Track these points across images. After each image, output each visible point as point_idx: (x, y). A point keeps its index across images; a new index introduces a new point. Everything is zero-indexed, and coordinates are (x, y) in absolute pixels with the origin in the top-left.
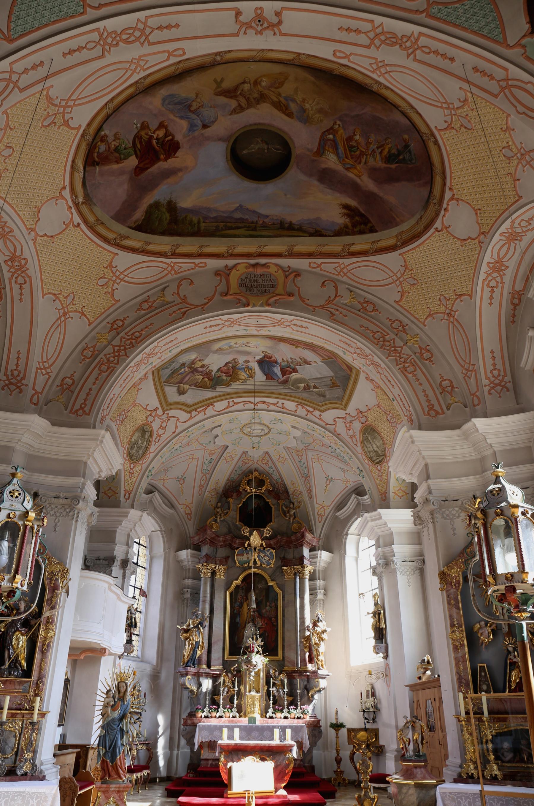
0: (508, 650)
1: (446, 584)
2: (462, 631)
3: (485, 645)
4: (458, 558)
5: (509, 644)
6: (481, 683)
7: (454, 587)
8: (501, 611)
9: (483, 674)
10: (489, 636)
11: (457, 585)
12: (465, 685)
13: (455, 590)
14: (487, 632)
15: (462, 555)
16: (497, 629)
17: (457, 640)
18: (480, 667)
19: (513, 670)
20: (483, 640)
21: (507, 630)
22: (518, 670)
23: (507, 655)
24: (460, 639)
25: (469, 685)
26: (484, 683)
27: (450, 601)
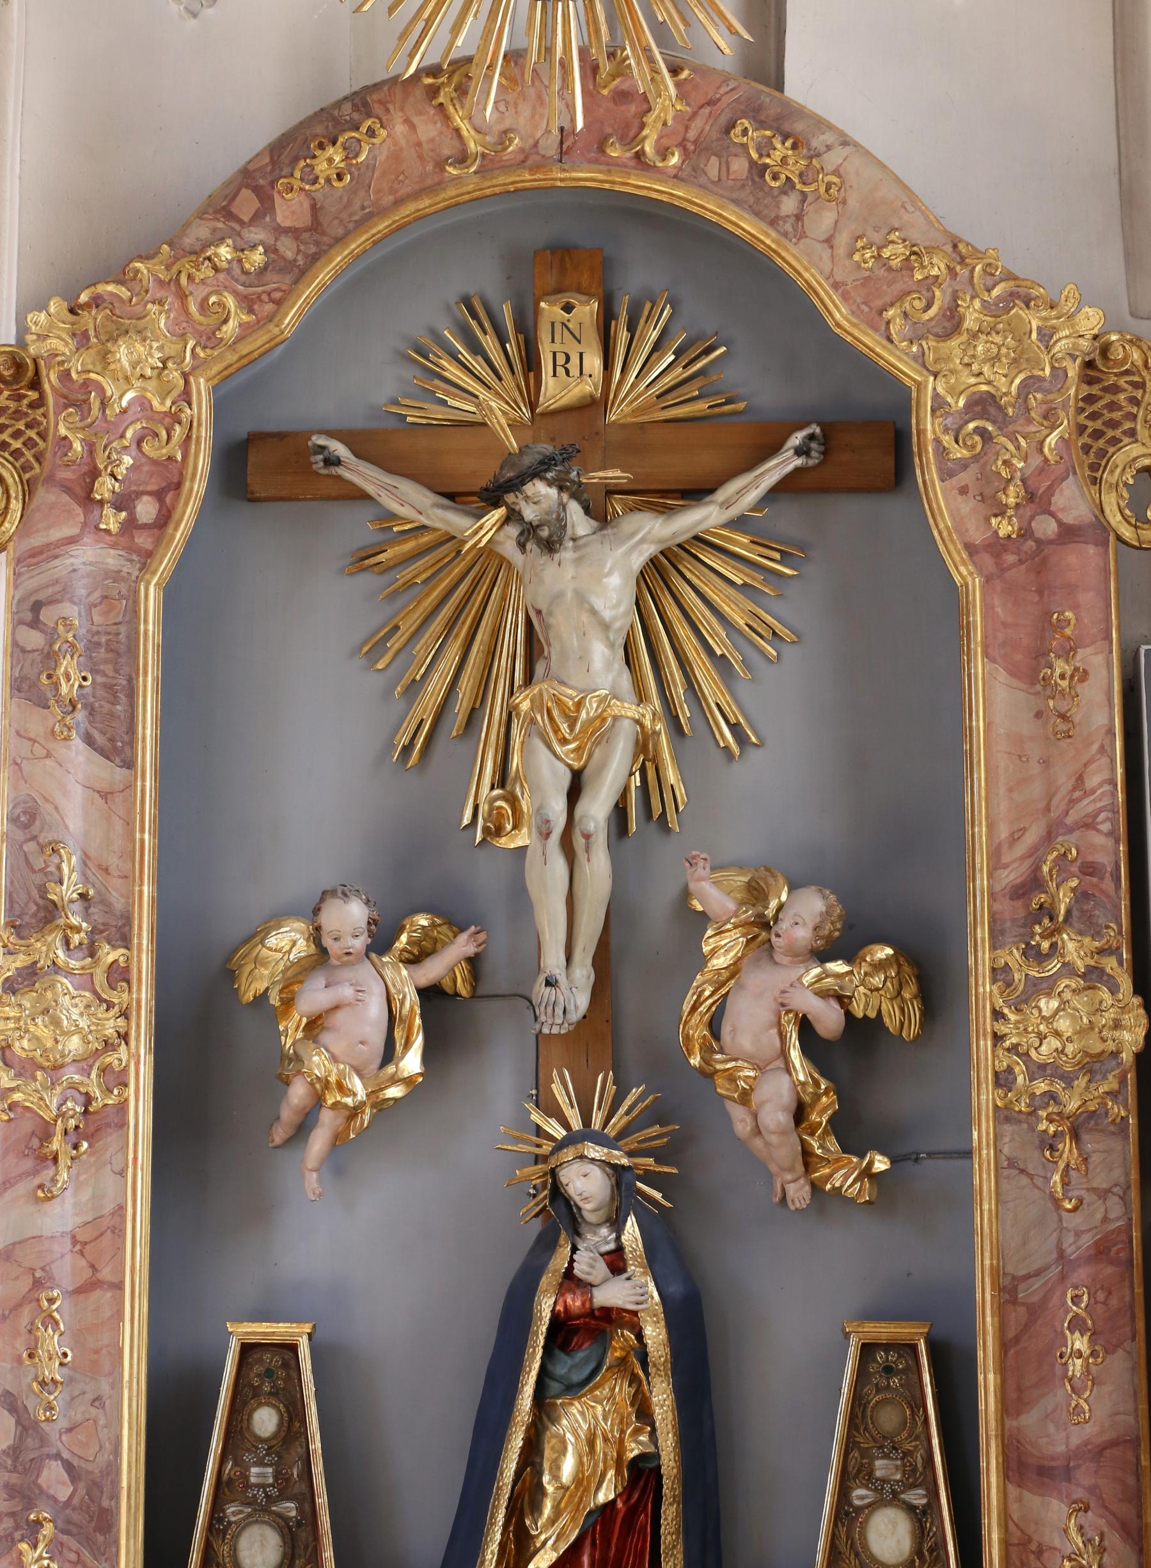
0: (557, 1193)
1: (29, 489)
2: (120, 975)
3: (338, 1141)
4: (202, 231)
5: (572, 1139)
6: (233, 1511)
7: (112, 520)
8: (557, 806)
9: (265, 1421)
10: (389, 1055)
11: (146, 510)
12: (66, 1528)
13: (112, 559)
14: (375, 1009)
15: (247, 203)
16: (474, 996)
17: (57, 1068)
18: (247, 1349)
19: (574, 1389)
20: (319, 1092)
21: (581, 1001)
22: (623, 1390)
23: (546, 1244)
24: (84, 1062)
25: (106, 1522)
26: (262, 1510)
27: (50, 657)
